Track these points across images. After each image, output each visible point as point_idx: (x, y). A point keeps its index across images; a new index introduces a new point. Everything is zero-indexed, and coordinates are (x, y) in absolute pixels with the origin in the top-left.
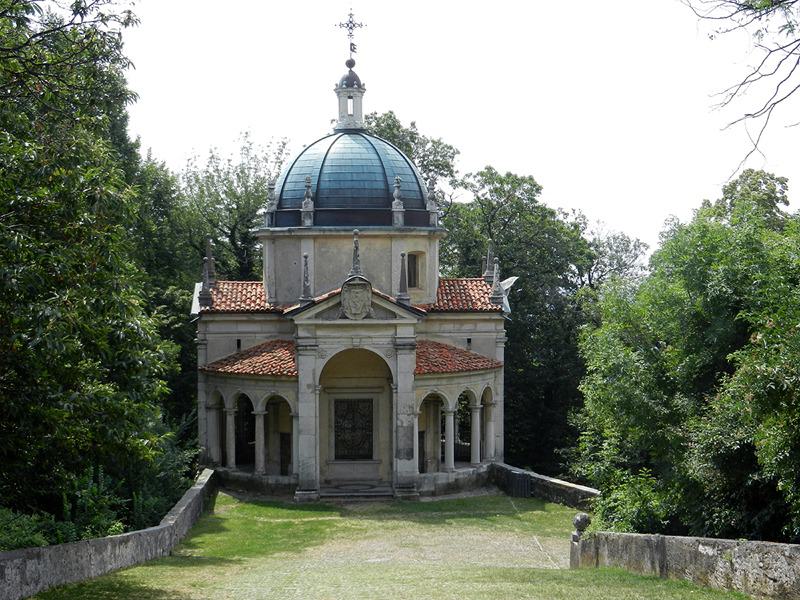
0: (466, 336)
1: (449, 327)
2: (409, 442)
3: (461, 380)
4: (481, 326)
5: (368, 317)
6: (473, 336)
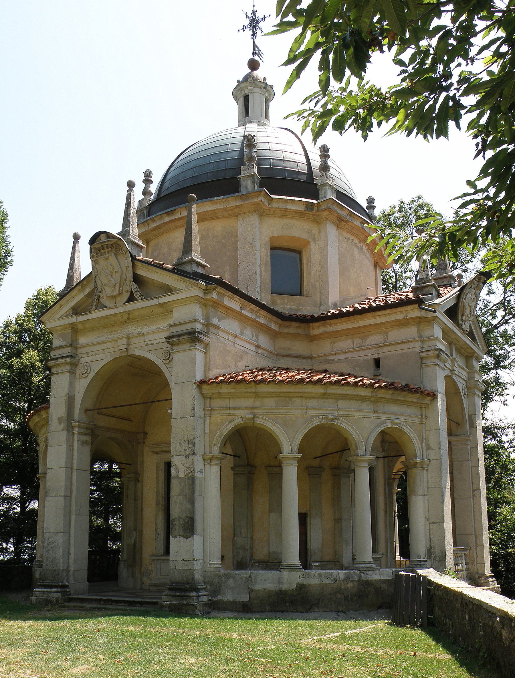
0: (371, 355)
1: (345, 344)
2: (189, 506)
3: (311, 403)
4: (395, 335)
5: (131, 299)
6: (383, 353)
